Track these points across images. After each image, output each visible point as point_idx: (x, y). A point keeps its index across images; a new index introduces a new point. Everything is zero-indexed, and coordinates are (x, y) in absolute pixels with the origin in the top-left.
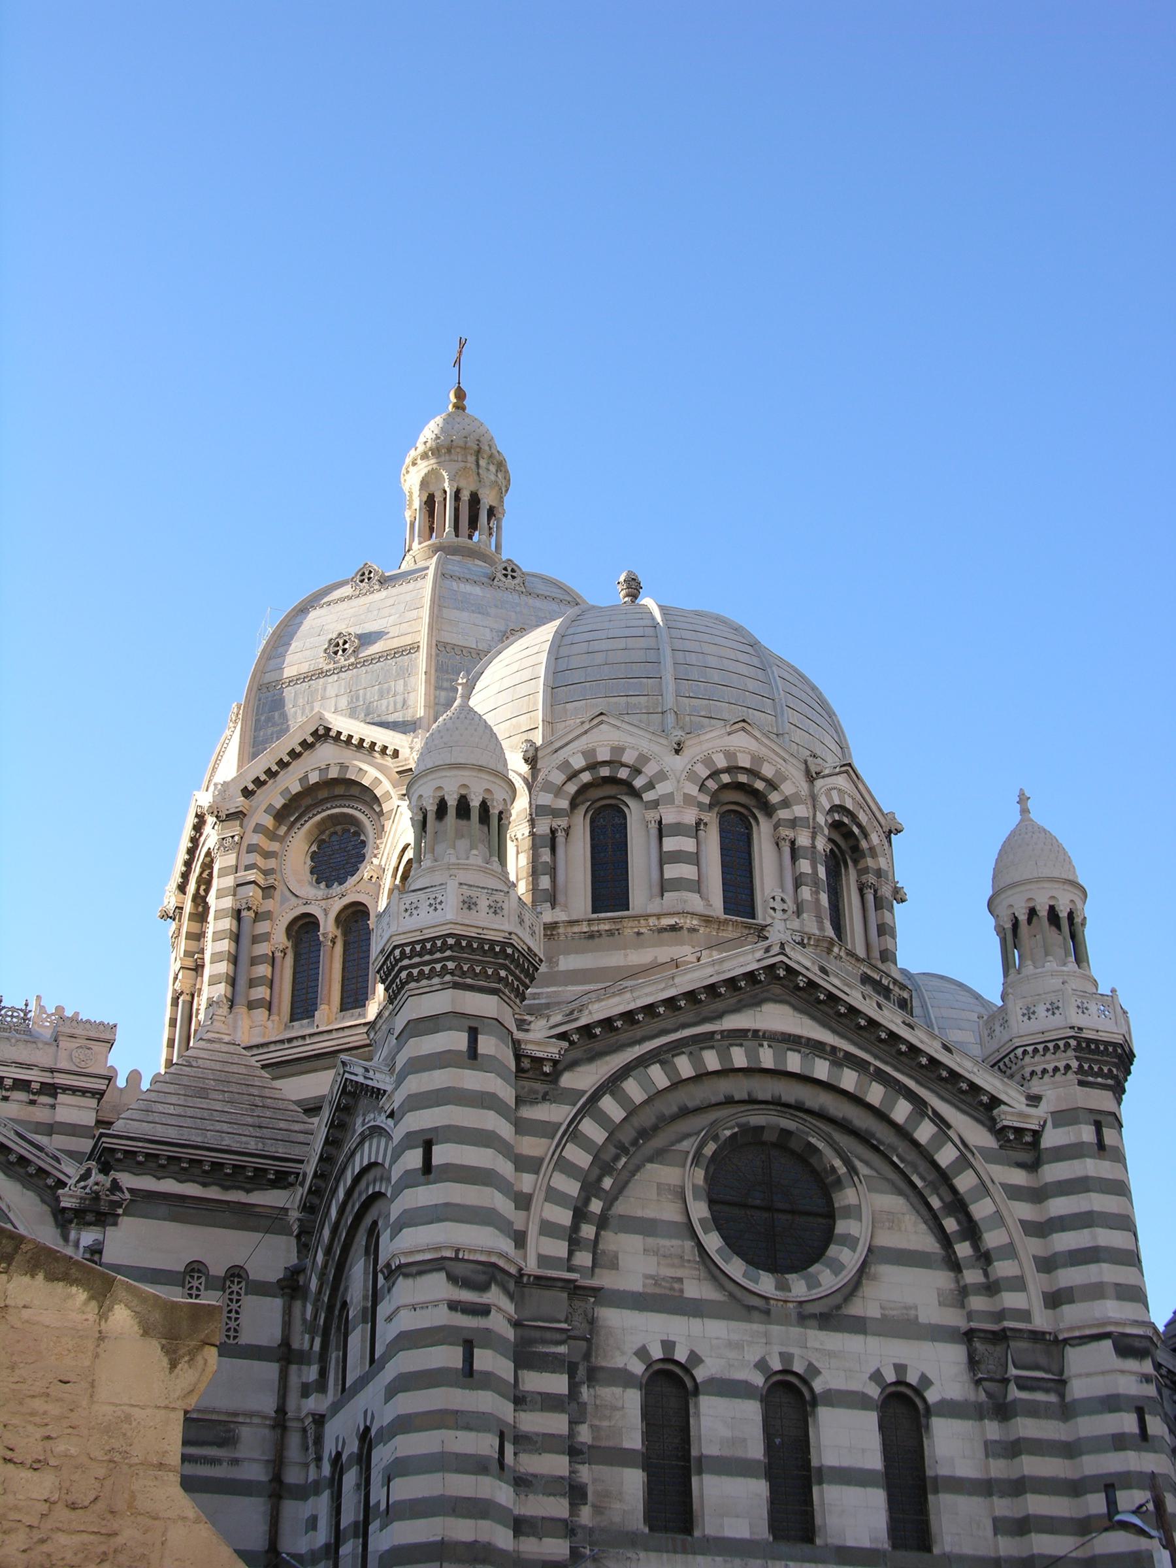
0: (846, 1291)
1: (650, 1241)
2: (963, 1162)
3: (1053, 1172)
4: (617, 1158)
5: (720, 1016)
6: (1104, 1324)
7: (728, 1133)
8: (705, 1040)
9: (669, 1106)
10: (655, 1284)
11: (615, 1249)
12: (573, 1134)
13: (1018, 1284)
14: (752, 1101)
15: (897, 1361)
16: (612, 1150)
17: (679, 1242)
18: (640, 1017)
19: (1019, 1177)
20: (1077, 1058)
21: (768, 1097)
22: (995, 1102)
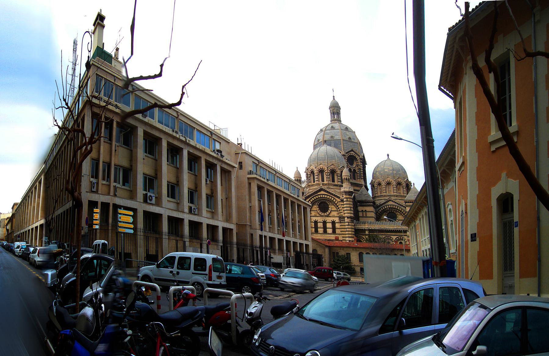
2: (338, 203)
5: (318, 193)
8: (316, 195)
9: (315, 201)
13: (342, 212)
19: (342, 203)
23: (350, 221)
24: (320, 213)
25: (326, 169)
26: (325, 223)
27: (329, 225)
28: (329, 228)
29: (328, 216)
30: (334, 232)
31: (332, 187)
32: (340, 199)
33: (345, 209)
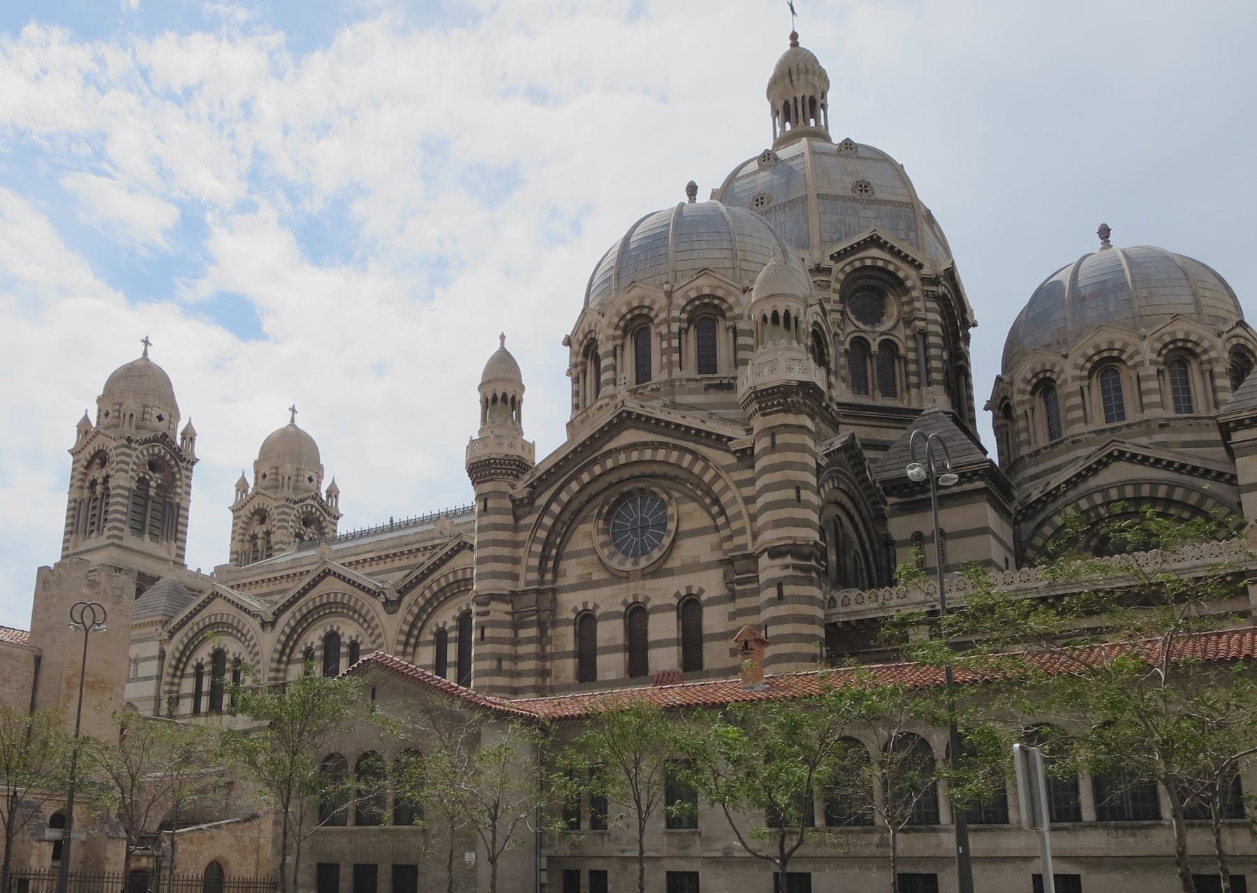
0: (664, 557)
1: (580, 559)
2: (717, 477)
3: (759, 465)
4: (563, 528)
7: (614, 499)
9: (584, 497)
13: (742, 531)
14: (621, 481)
17: (590, 557)
18: (562, 463)
19: (747, 474)
20: (758, 403)
21: (628, 476)
24: (614, 563)
26: (636, 615)
27: (663, 626)
28: (661, 644)
29: (657, 571)
32: (728, 451)
33: (760, 502)
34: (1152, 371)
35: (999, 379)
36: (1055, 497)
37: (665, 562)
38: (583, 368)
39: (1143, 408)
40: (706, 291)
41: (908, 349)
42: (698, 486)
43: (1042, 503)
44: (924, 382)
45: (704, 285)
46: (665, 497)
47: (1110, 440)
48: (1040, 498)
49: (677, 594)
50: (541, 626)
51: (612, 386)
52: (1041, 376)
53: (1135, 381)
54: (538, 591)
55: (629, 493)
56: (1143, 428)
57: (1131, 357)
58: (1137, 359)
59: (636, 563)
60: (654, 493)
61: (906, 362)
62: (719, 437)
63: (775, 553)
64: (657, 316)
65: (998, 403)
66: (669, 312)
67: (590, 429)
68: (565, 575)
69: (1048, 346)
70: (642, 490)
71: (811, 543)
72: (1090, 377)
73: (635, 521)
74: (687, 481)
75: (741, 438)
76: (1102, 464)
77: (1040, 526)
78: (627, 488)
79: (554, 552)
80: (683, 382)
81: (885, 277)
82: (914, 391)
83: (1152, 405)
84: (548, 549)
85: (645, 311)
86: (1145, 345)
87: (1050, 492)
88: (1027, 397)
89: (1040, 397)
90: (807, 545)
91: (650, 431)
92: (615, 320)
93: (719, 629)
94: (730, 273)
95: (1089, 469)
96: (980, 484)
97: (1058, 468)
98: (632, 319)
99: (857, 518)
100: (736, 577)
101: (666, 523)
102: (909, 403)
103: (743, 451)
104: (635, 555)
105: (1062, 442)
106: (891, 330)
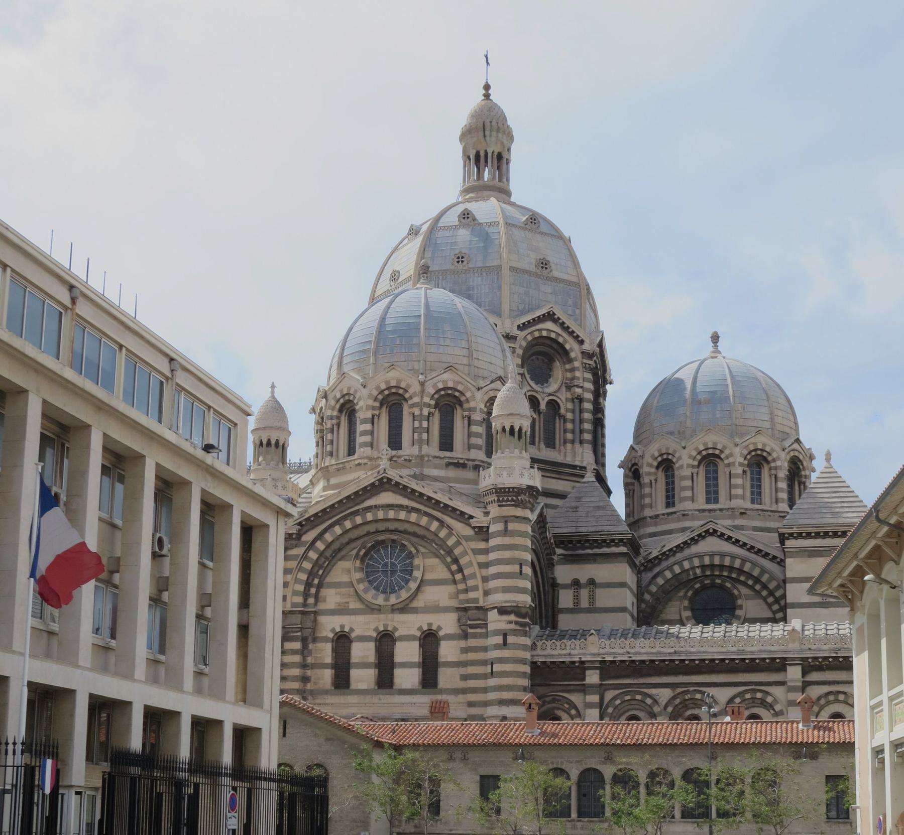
0: (411, 598)
1: (338, 590)
2: (458, 543)
3: (493, 542)
4: (325, 562)
5: (363, 501)
6: (494, 604)
7: (370, 545)
8: (356, 513)
9: (345, 540)
10: (339, 605)
11: (325, 595)
12: (305, 557)
13: (475, 588)
15: (428, 622)
16: (323, 560)
17: (347, 589)
19: (482, 545)
21: (384, 529)
22: (471, 517)
23: (513, 626)
24: (369, 596)
25: (415, 388)
28: (404, 665)
29: (404, 608)
30: (429, 680)
31: (435, 472)
32: (469, 525)
33: (492, 570)
34: (739, 470)
35: (632, 448)
36: (668, 557)
37: (411, 601)
38: (338, 421)
39: (731, 497)
40: (450, 385)
41: (567, 410)
42: (441, 547)
43: (658, 560)
44: (577, 440)
45: (449, 380)
46: (413, 549)
47: (708, 520)
48: (657, 556)
49: (420, 628)
50: (304, 641)
51: (370, 448)
52: (665, 456)
53: (728, 476)
54: (303, 613)
55: (383, 542)
56: (730, 513)
57: (727, 457)
58: (731, 460)
59: (387, 600)
60: (403, 545)
61: (565, 420)
62: (462, 514)
63: (503, 611)
64: (411, 398)
65: (630, 466)
66: (422, 397)
67: (355, 486)
68: (325, 601)
69: (672, 433)
70: (394, 541)
71: (528, 606)
72: (698, 466)
73: (386, 565)
74: (433, 541)
75: (480, 518)
76: (701, 537)
77: (655, 577)
78: (381, 538)
79: (316, 581)
80: (431, 458)
81: (555, 346)
82: (569, 446)
83: (737, 497)
84: (311, 577)
85: (401, 391)
86: (737, 451)
87: (665, 552)
88: (653, 470)
89: (662, 471)
90: (525, 607)
91: (405, 496)
92: (375, 393)
93: (451, 659)
94: (466, 369)
95: (692, 539)
96: (623, 549)
97: (670, 532)
98: (388, 395)
99: (538, 568)
100: (469, 622)
101: (412, 570)
102: (565, 456)
103: (481, 528)
104: (384, 592)
105: (675, 513)
106: (555, 392)
